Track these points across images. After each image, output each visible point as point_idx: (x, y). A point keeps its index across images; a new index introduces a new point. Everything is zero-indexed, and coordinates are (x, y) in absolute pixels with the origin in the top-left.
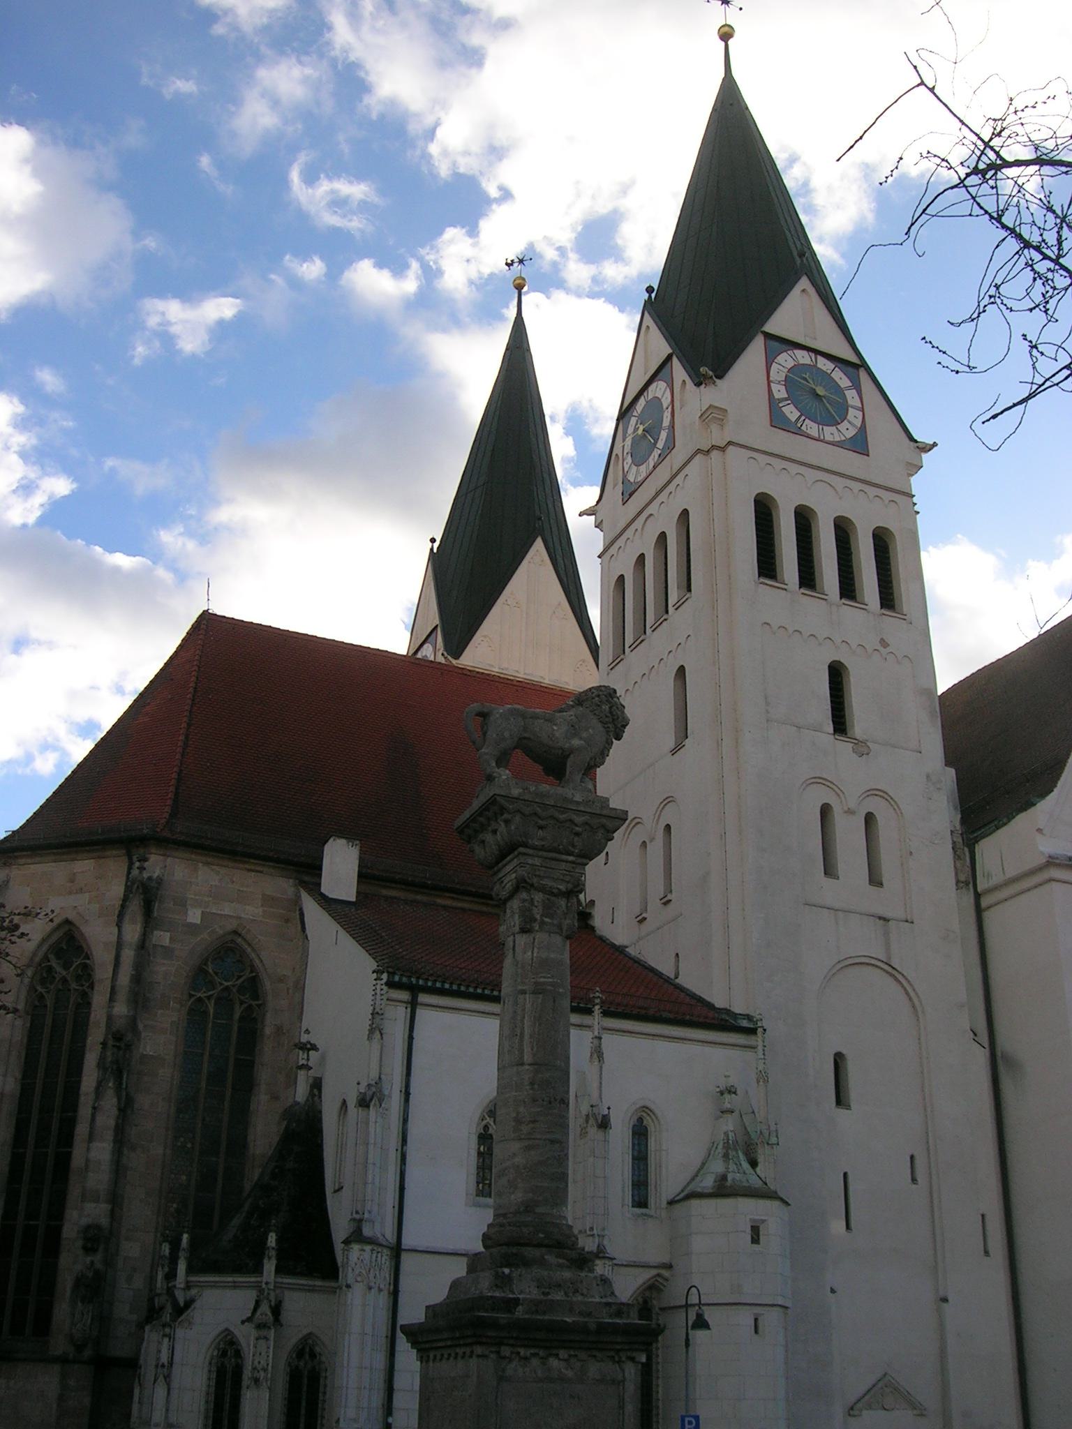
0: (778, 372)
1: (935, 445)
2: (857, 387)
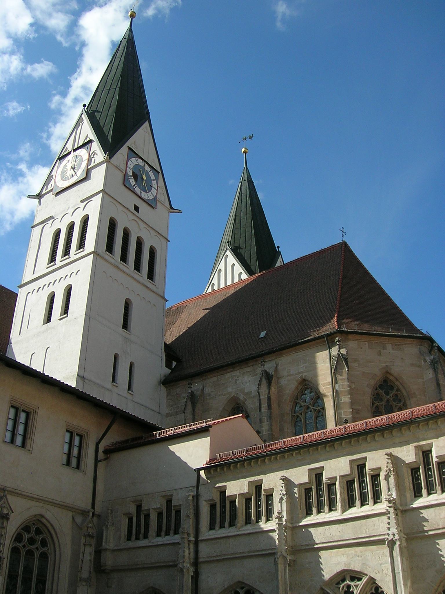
0: (131, 165)
1: (179, 211)
2: (157, 180)
